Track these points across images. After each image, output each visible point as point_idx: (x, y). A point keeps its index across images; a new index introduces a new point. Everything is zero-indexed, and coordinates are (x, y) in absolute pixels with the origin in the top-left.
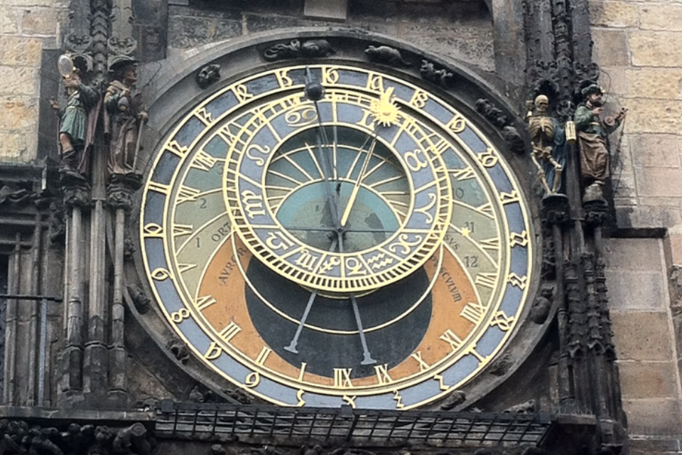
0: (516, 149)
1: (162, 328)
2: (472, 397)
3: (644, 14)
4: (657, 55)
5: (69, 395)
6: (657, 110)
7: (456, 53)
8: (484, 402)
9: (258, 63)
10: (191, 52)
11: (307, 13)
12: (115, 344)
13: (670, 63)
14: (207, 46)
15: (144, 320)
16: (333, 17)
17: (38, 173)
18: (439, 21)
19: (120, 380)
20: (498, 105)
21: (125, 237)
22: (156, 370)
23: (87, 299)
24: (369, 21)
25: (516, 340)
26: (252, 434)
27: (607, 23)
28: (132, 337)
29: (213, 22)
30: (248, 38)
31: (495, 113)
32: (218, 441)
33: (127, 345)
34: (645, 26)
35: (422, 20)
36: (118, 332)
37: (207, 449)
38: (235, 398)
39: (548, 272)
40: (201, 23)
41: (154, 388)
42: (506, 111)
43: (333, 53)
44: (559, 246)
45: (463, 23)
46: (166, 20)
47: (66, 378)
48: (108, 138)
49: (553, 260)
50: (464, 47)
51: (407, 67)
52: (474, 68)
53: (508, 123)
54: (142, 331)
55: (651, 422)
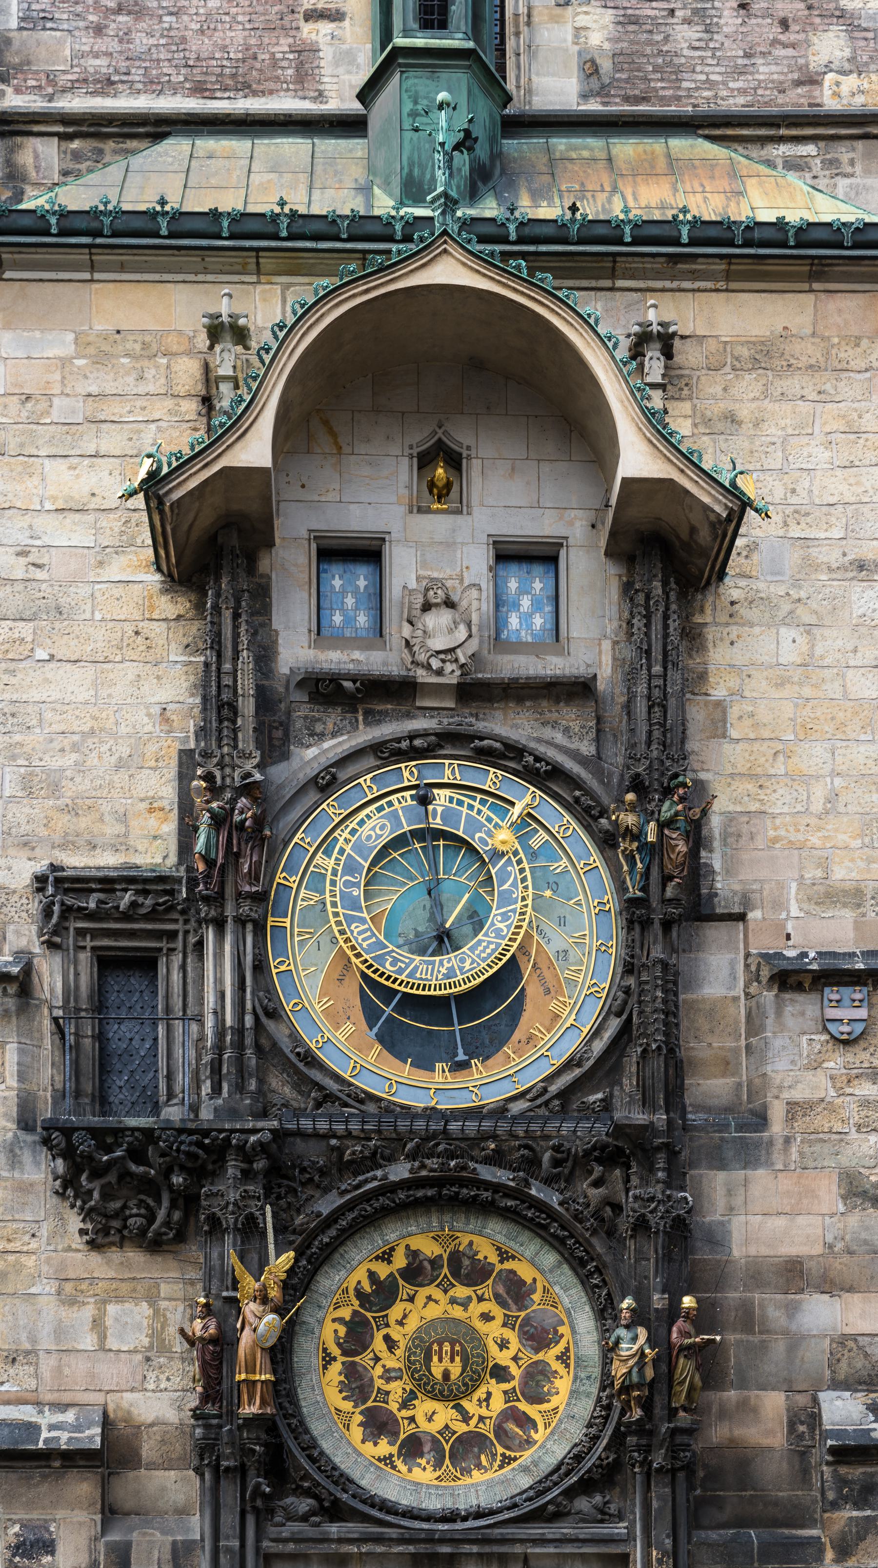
0: (607, 842)
1: (287, 1032)
2: (553, 1089)
3: (747, 680)
4: (756, 726)
5: (211, 1099)
6: (750, 787)
7: (559, 738)
8: (564, 1095)
9: (372, 762)
10: (311, 752)
11: (418, 704)
12: (248, 1051)
13: (766, 734)
14: (326, 745)
15: (270, 1025)
16: (443, 705)
17: (179, 881)
18: (545, 703)
19: (253, 1085)
20: (593, 798)
21: (254, 947)
22: (284, 1070)
23: (223, 1007)
24: (478, 707)
25: (596, 1033)
26: (363, 1130)
27: (711, 692)
28: (263, 1041)
29: (333, 718)
30: (366, 735)
31: (590, 807)
32: (335, 1136)
33: (258, 1048)
34: (747, 693)
35: (528, 704)
36: (249, 1040)
37: (324, 1143)
38: (349, 1096)
39: (629, 968)
40: (319, 720)
41: (281, 1088)
42: (599, 803)
43: (442, 747)
44: (638, 944)
45: (567, 704)
46: (288, 713)
47: (208, 1083)
48: (238, 855)
49: (632, 957)
50: (566, 730)
51: (511, 759)
52: (575, 755)
53: (601, 816)
54: (270, 1037)
55: (716, 1102)
